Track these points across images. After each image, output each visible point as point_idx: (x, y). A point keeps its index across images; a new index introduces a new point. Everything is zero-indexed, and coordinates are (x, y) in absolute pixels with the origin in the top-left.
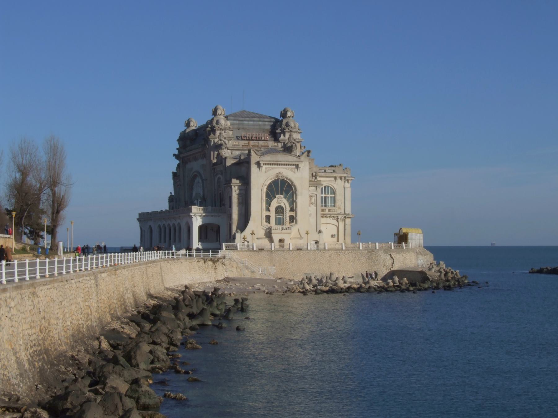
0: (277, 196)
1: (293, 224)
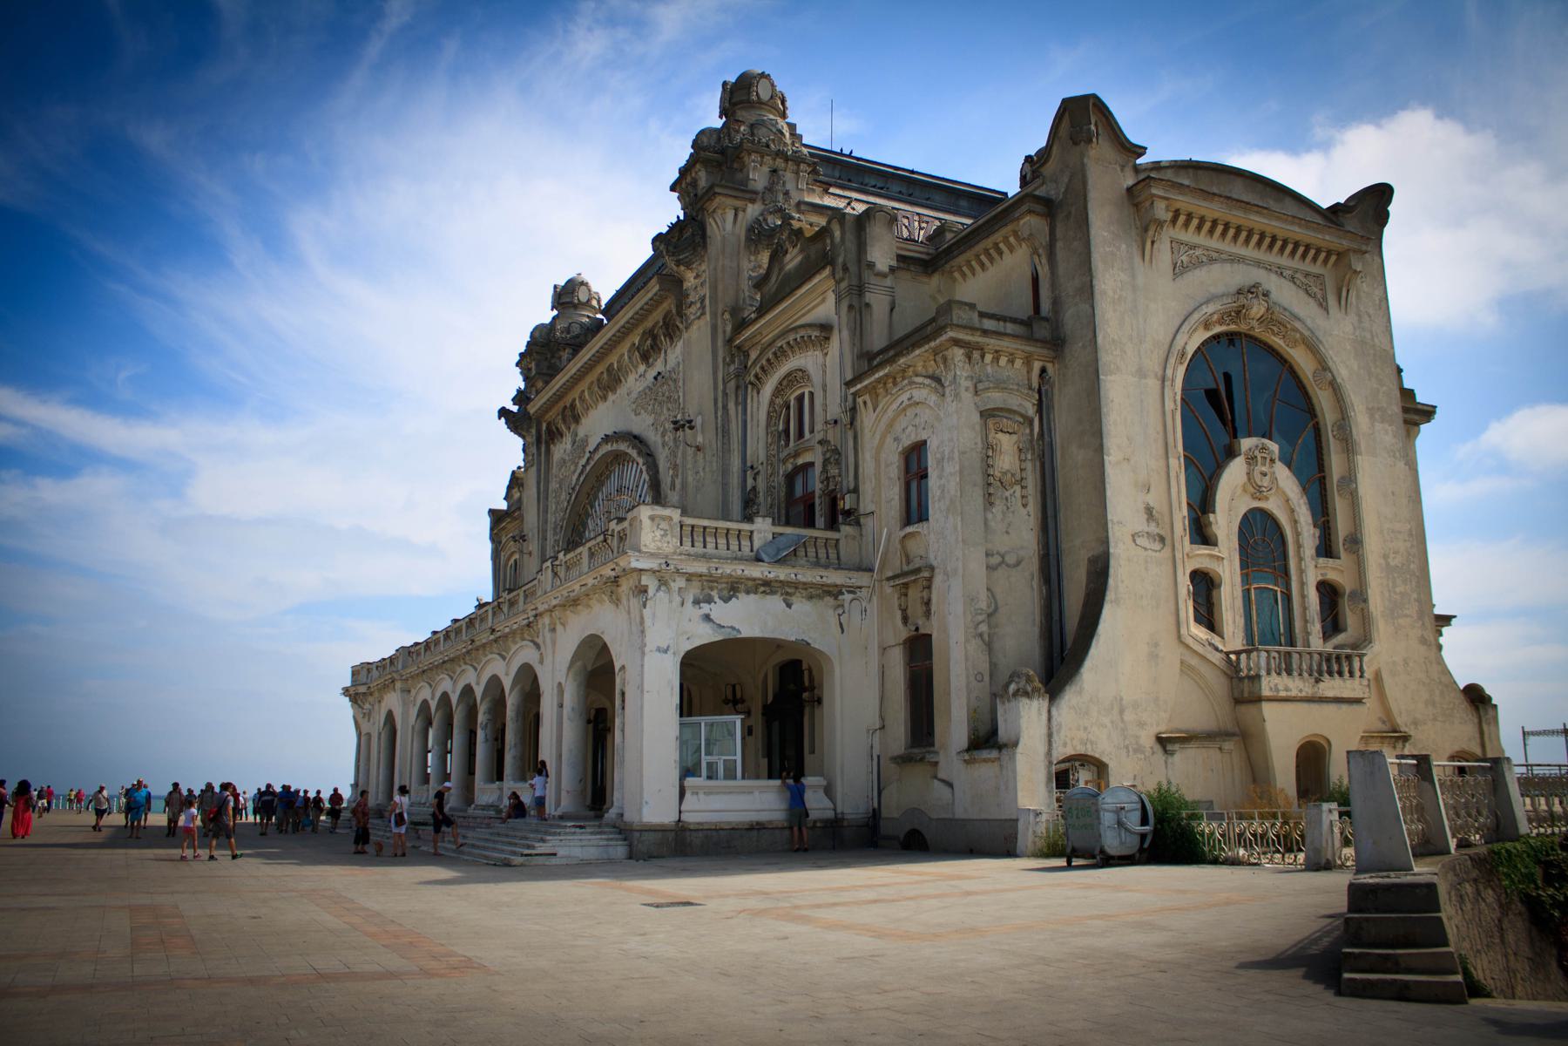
0: (1246, 443)
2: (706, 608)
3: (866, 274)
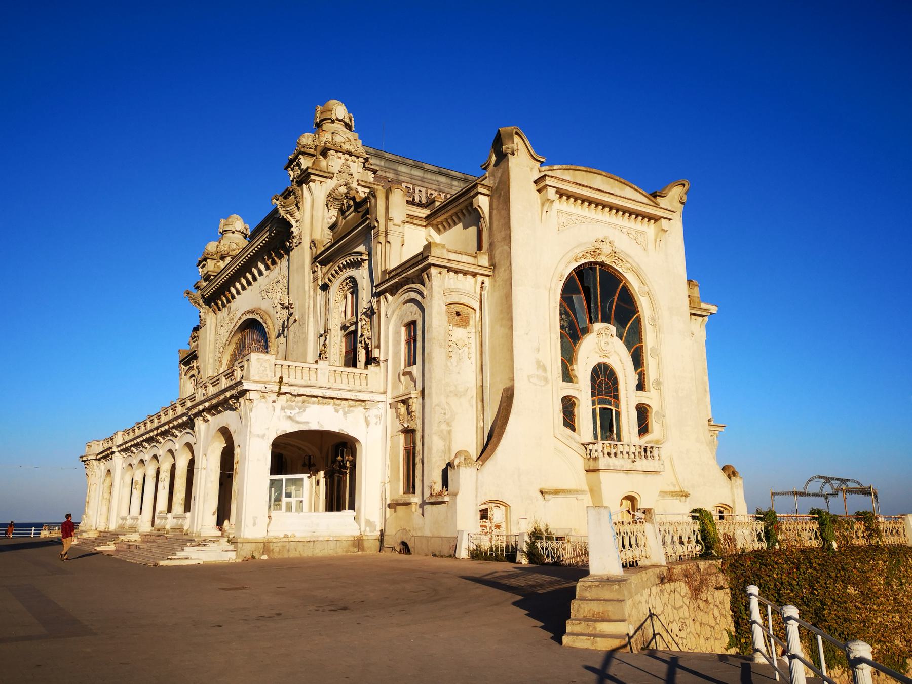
0: (598, 326)
1: (648, 437)
2: (288, 412)
3: (390, 224)
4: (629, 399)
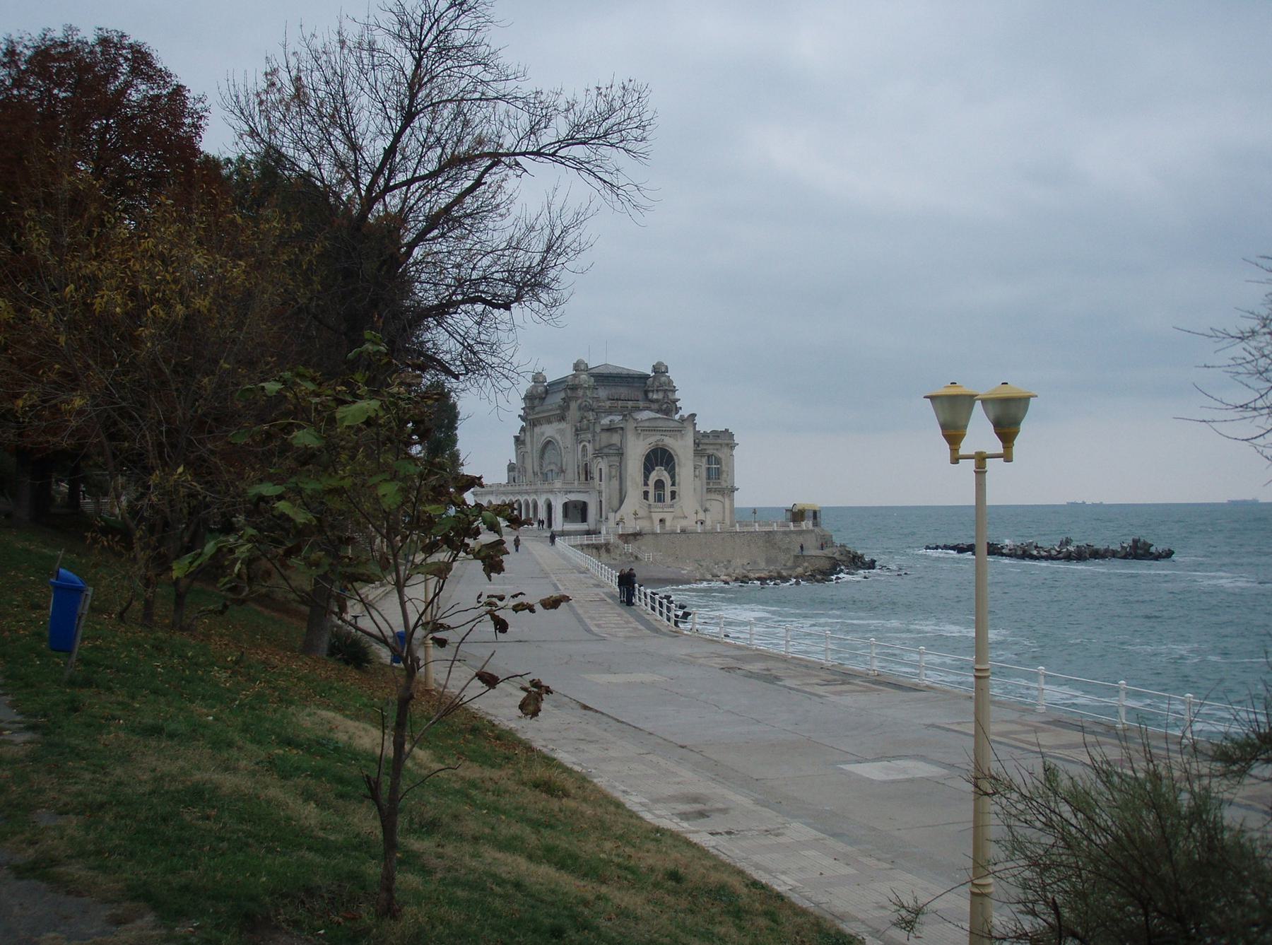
4: (668, 488)
